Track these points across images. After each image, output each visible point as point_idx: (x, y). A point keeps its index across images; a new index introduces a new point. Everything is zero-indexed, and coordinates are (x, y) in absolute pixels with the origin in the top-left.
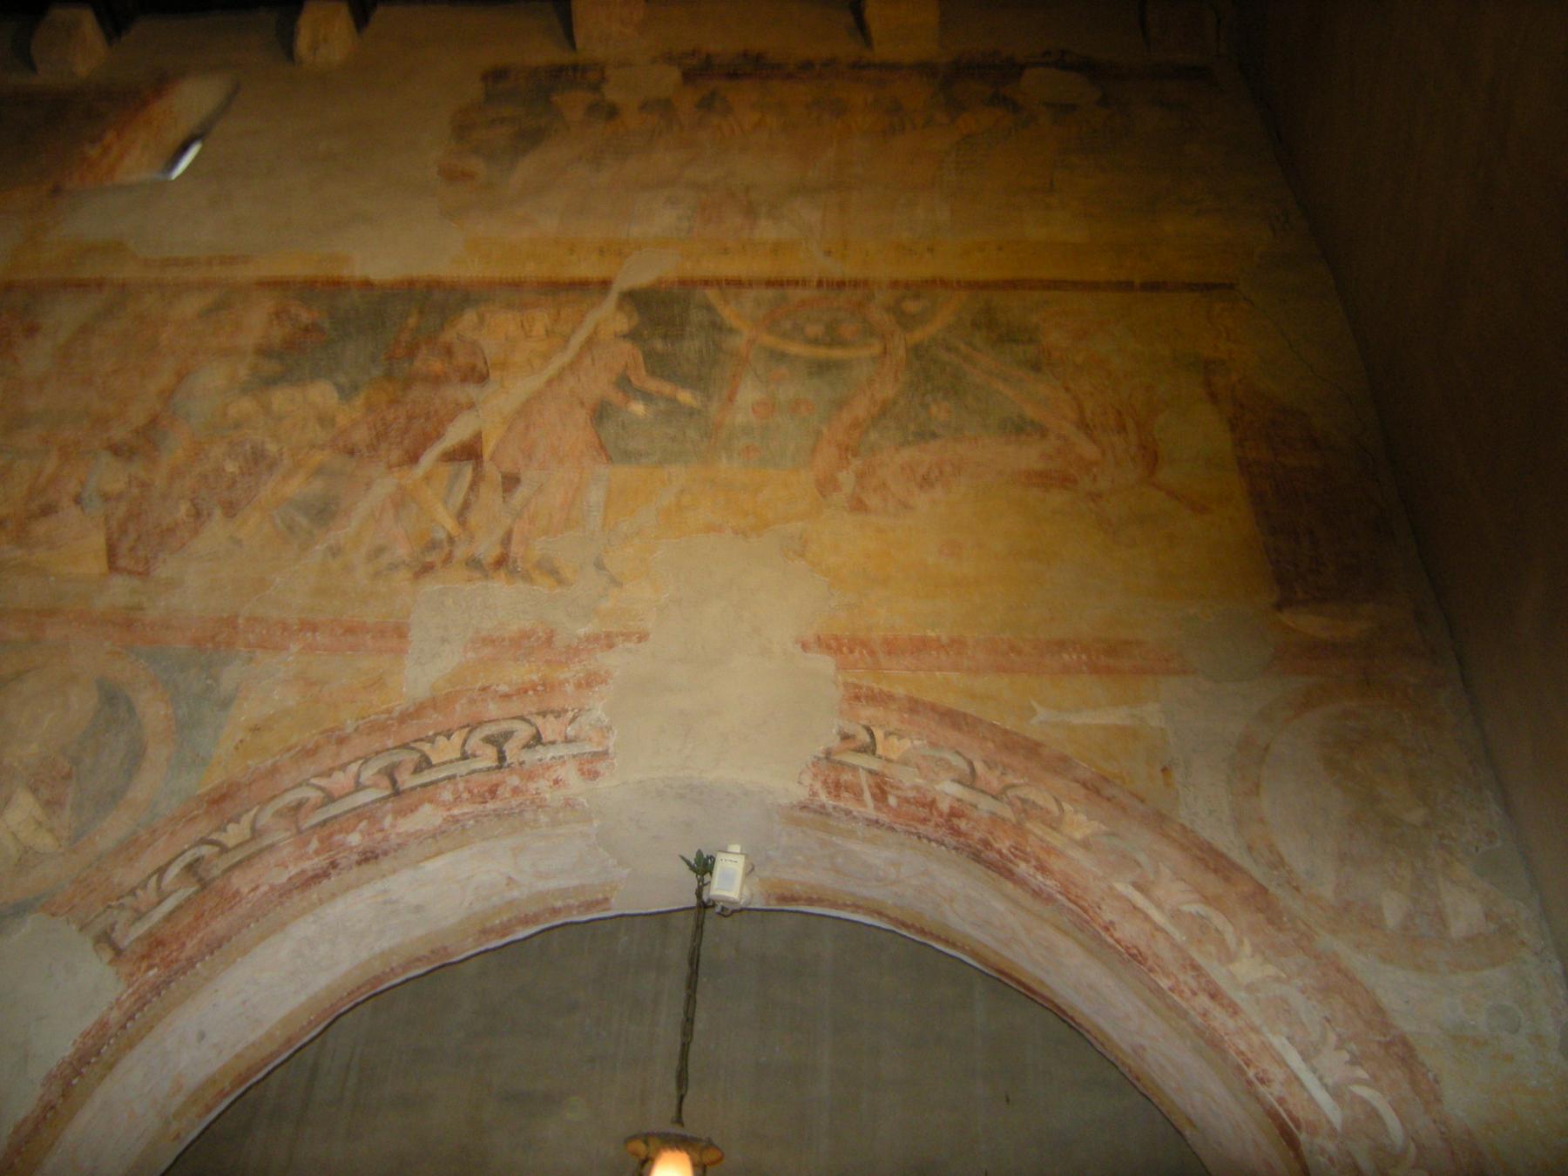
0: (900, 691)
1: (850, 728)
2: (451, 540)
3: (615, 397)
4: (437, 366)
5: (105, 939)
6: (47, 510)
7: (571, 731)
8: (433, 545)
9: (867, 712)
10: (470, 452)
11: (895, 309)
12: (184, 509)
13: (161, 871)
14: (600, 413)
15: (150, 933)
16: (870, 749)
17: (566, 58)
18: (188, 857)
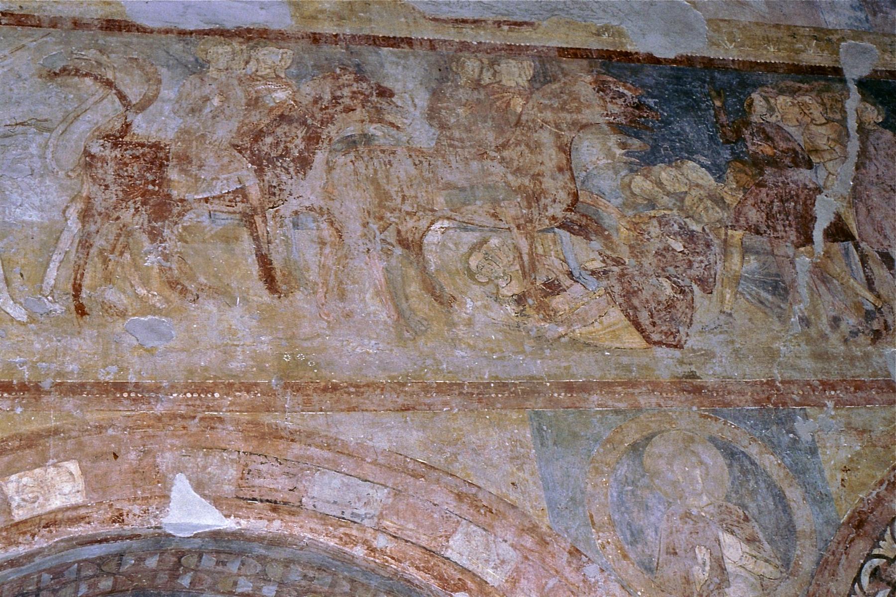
6: (553, 288)
8: (869, 316)
10: (838, 232)
12: (666, 284)
13: (857, 579)
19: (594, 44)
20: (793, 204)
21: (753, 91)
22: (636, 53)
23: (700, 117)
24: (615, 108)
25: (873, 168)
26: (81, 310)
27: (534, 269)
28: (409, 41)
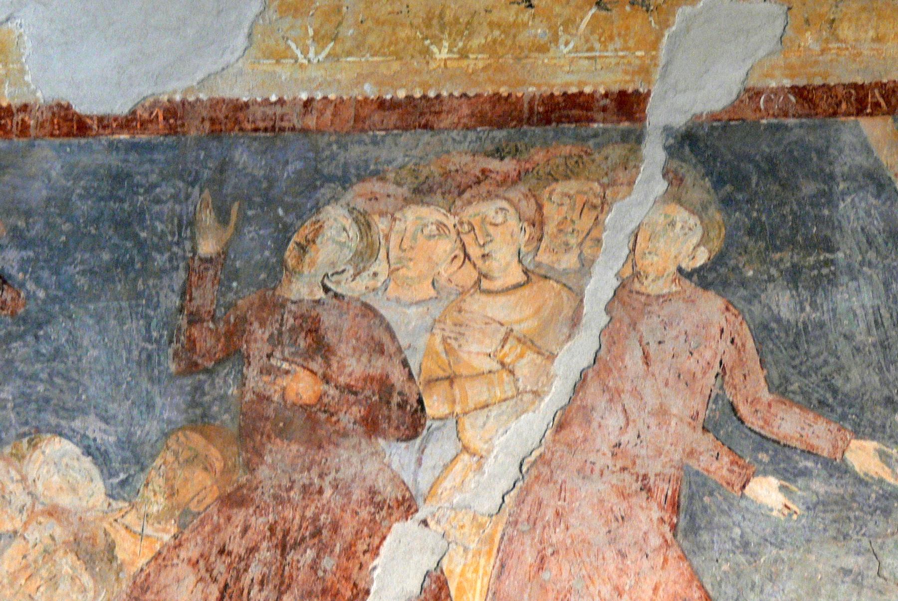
3: (716, 465)
4: (302, 386)
14: (689, 510)
20: (310, 554)
21: (335, 199)
22: (25, 108)
23: (139, 295)
25: (614, 421)
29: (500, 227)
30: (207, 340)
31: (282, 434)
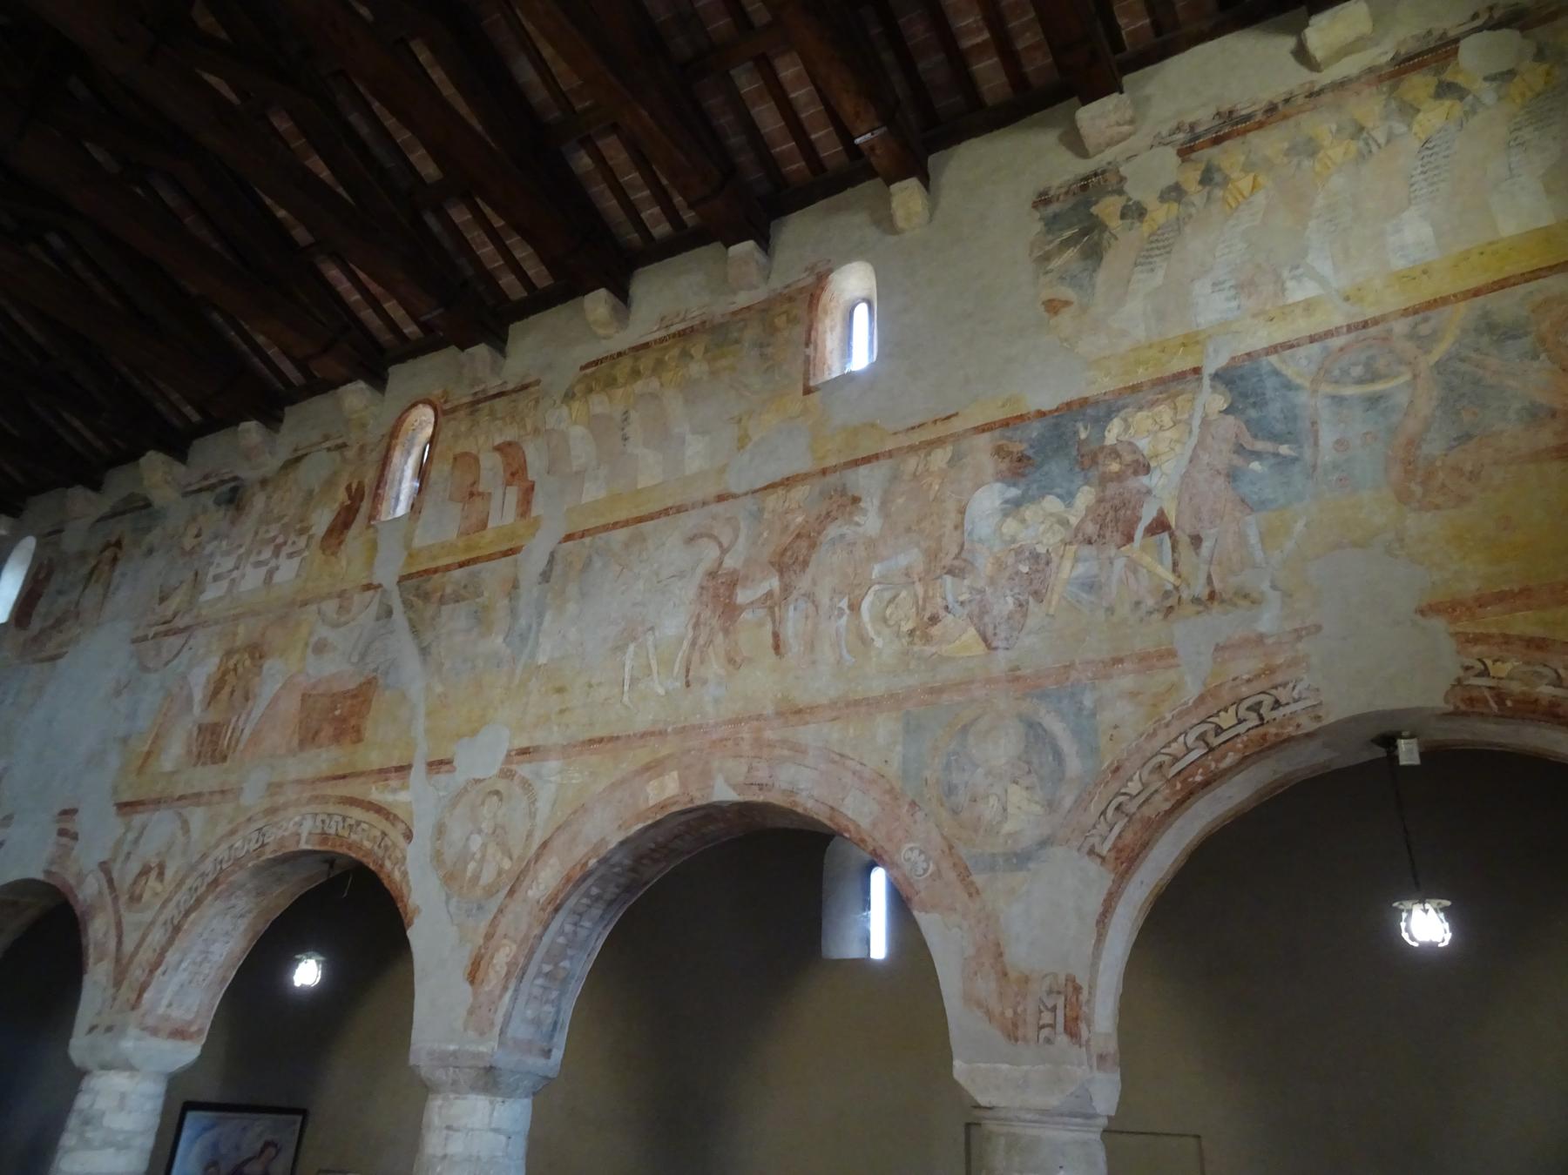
0: (1494, 630)
1: (1468, 662)
2: (1177, 588)
3: (1237, 461)
4: (1115, 467)
5: (1091, 852)
6: (934, 620)
7: (1295, 694)
8: (1167, 595)
9: (1477, 649)
10: (1160, 525)
11: (1412, 336)
13: (1103, 813)
15: (1114, 846)
16: (1485, 673)
17: (1083, 167)
18: (1114, 804)
19: (1000, 415)
24: (1004, 466)
26: (688, 684)
27: (924, 609)
28: (876, 457)
29: (1165, 413)
30: (1087, 461)
31: (1111, 480)
